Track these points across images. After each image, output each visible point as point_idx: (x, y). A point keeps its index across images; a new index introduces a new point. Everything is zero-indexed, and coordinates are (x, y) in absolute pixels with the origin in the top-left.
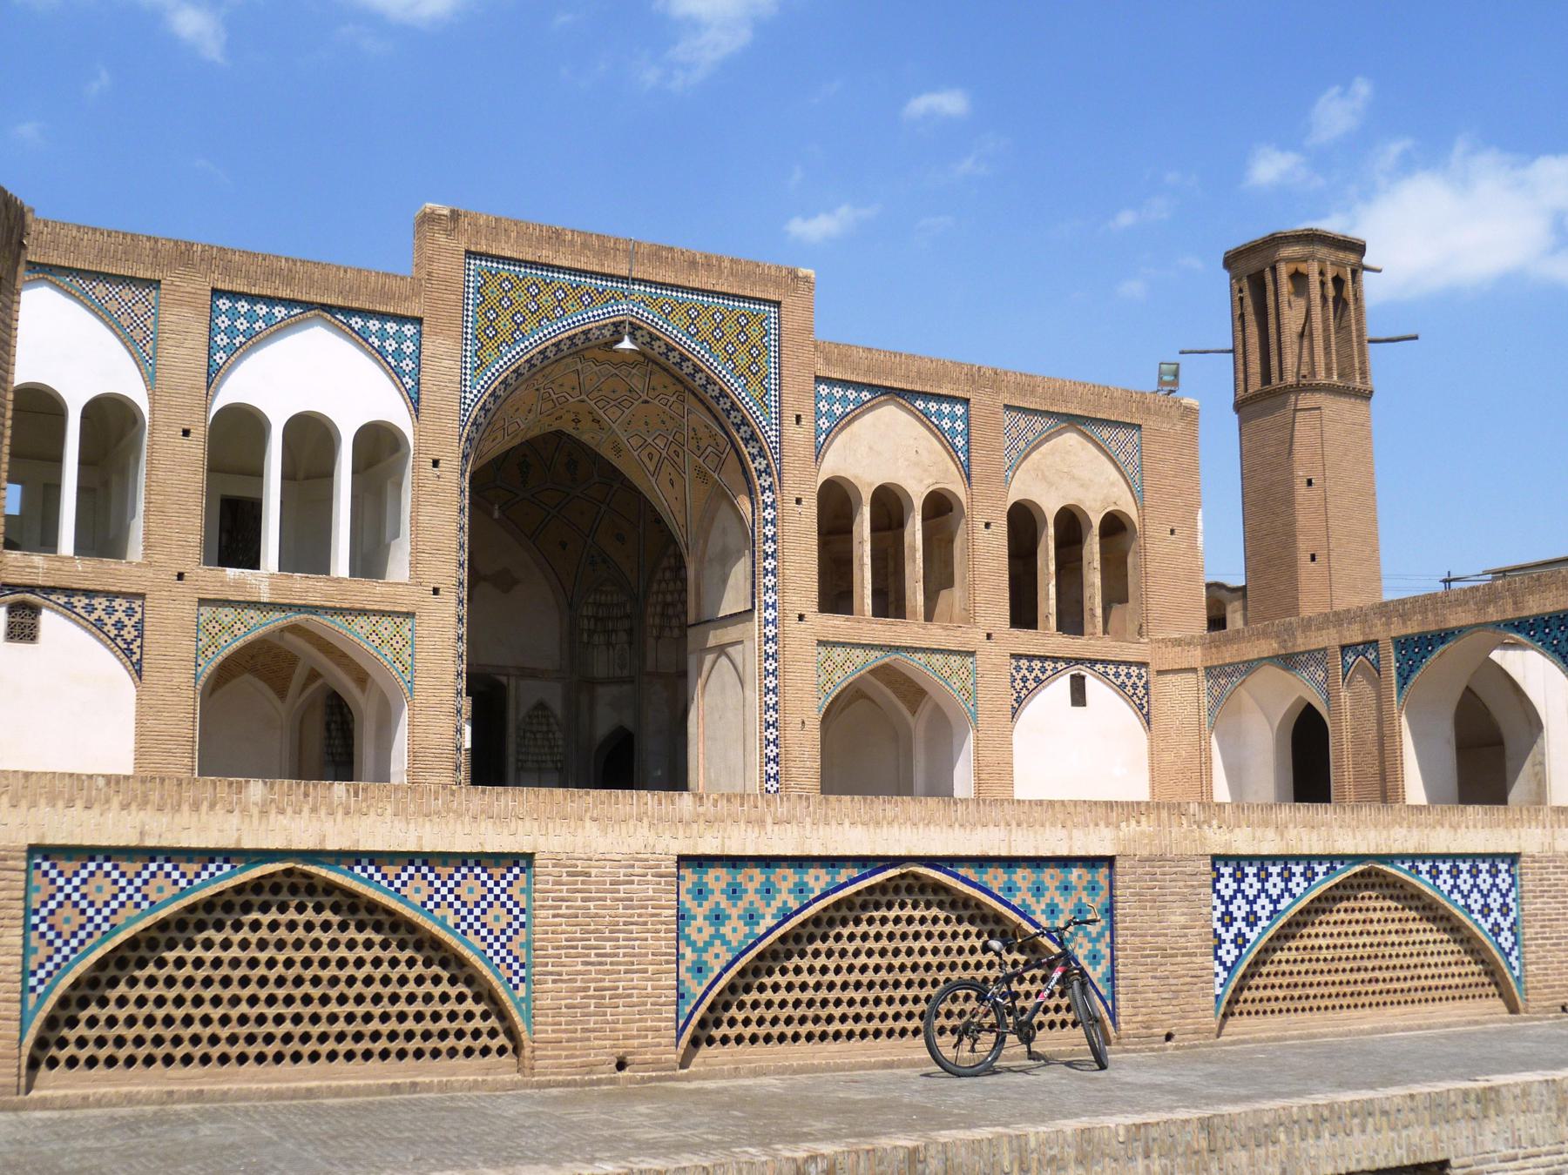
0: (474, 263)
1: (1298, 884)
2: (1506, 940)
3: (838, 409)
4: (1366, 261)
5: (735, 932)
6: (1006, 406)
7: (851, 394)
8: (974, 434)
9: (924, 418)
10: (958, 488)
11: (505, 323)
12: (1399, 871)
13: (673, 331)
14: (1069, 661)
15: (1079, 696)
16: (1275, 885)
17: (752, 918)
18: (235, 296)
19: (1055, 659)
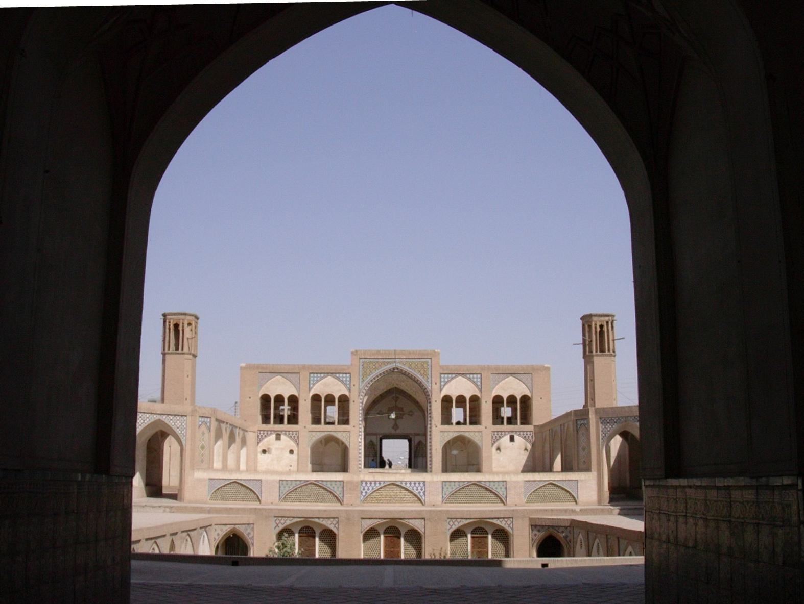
0: (361, 360)
1: (378, 485)
2: (422, 494)
3: (446, 380)
4: (615, 318)
5: (287, 489)
6: (492, 374)
7: (450, 376)
8: (483, 381)
9: (469, 379)
10: (478, 394)
11: (368, 371)
12: (399, 483)
13: (406, 368)
14: (509, 432)
15: (512, 439)
16: (373, 485)
17: (289, 487)
18: (313, 373)
19: (505, 432)
